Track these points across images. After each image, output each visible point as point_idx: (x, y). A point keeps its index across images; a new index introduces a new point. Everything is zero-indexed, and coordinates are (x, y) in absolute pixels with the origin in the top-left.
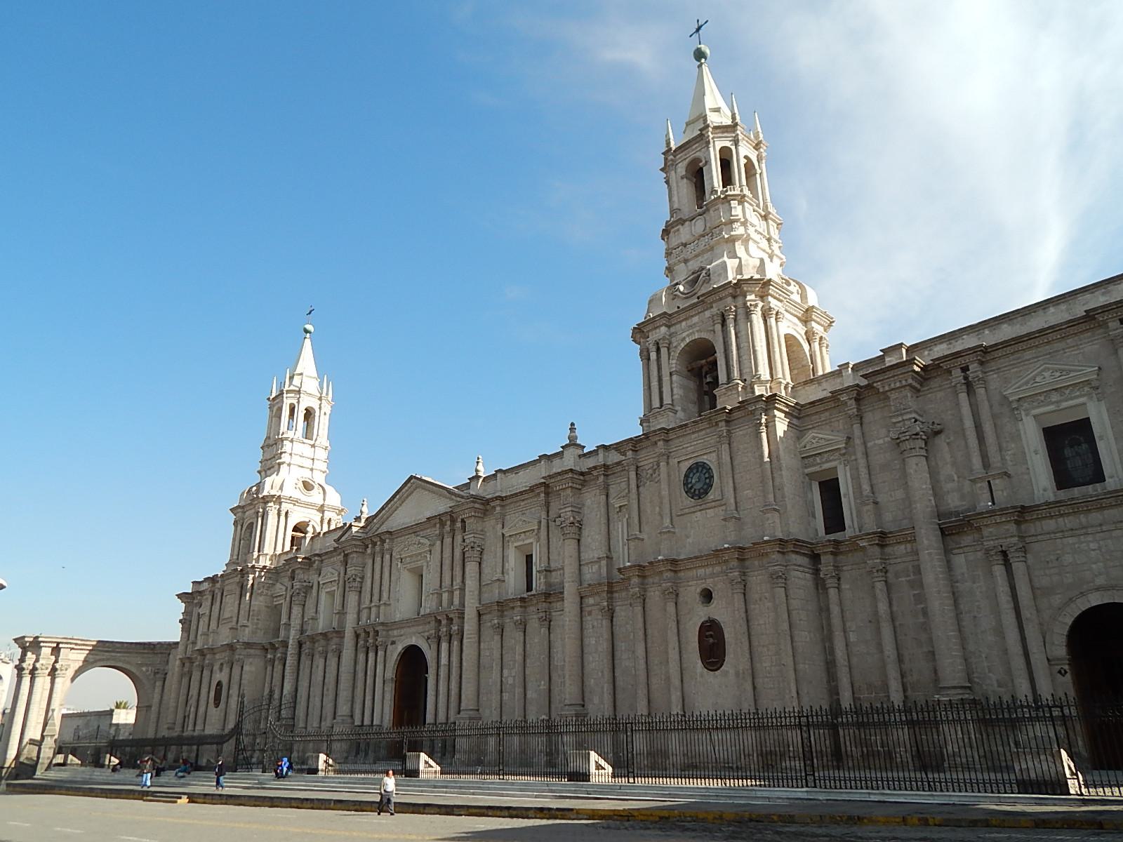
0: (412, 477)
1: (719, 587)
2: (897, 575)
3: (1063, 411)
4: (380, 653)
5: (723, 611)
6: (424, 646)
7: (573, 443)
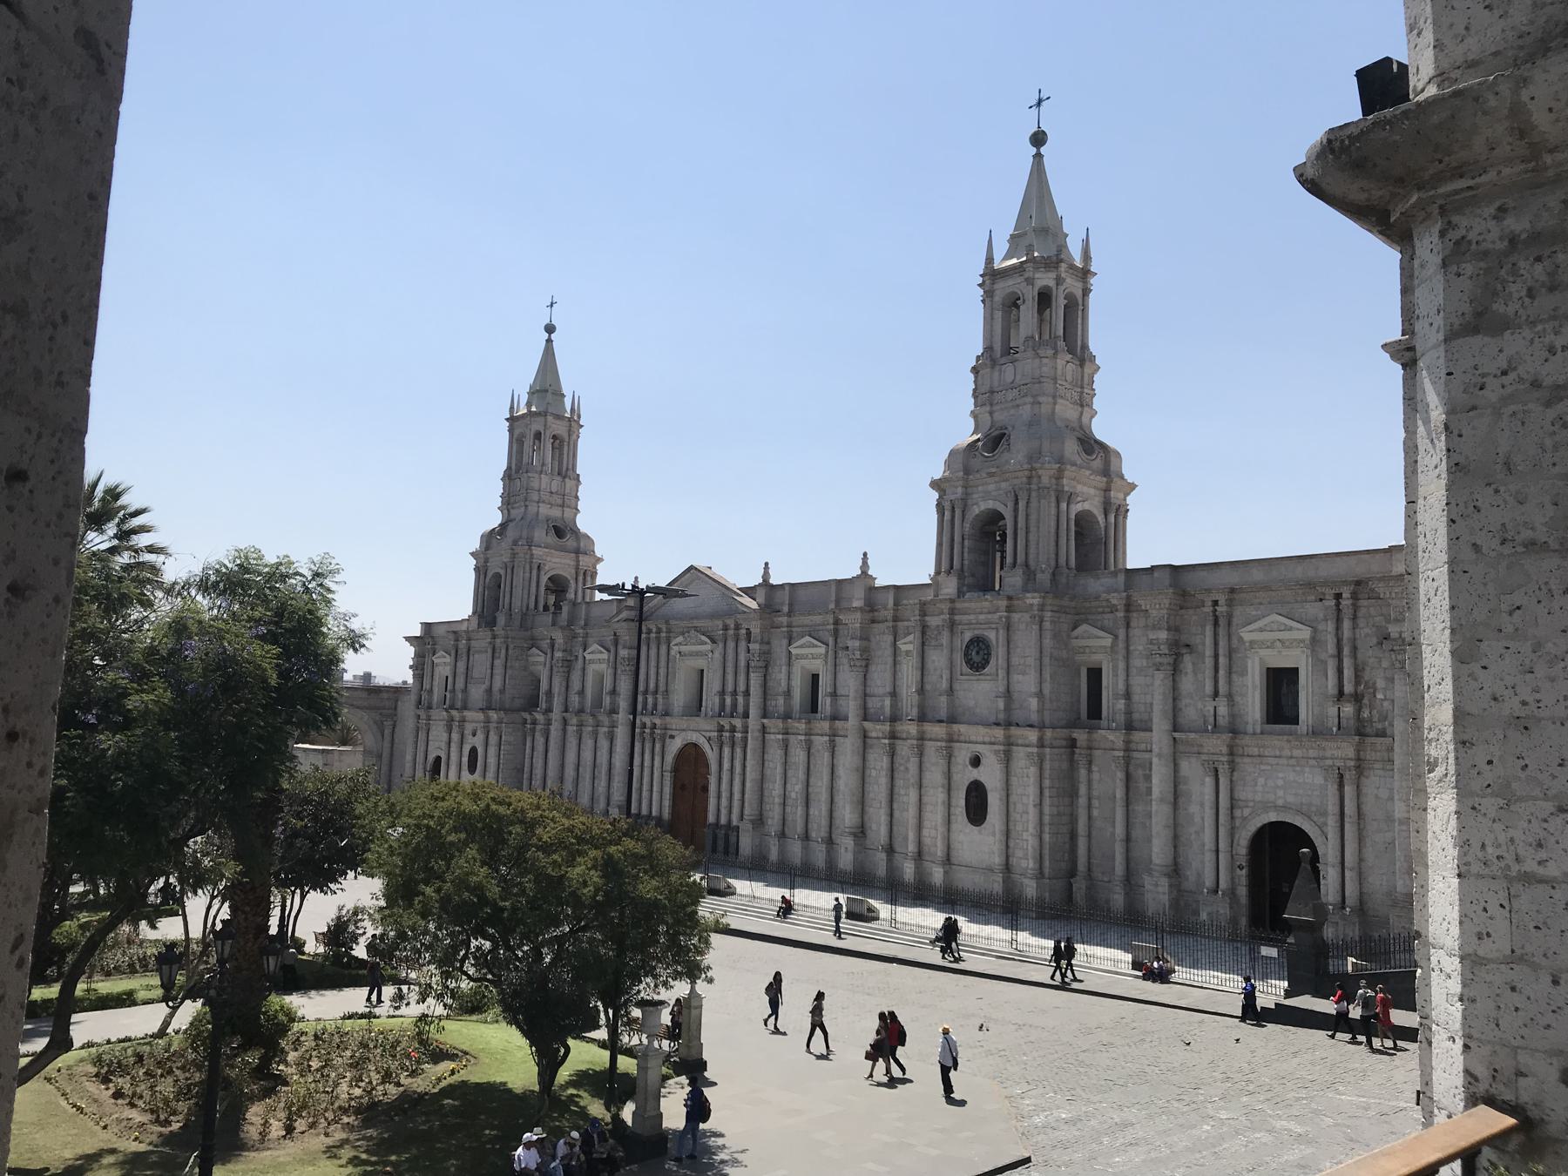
0: (692, 568)
5: (990, 775)
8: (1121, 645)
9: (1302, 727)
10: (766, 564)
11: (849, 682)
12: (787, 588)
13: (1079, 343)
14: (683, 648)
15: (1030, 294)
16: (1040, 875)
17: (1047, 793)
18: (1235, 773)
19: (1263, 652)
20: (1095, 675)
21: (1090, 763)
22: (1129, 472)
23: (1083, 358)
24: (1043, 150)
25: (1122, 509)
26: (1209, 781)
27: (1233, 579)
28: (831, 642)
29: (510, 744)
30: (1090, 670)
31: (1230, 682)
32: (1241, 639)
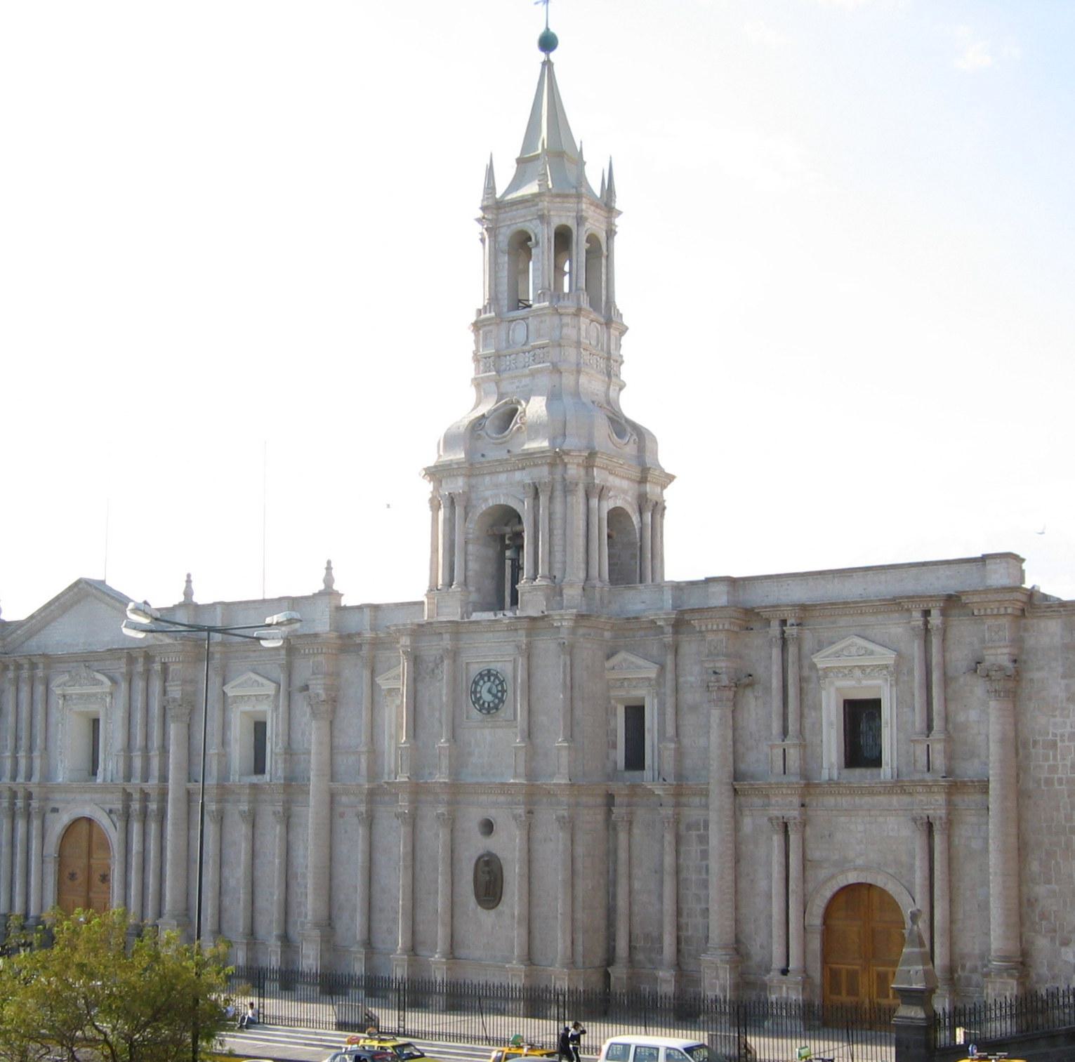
1: (500, 817)
2: (689, 828)
3: (862, 689)
4: (36, 823)
6: (104, 821)
7: (329, 592)
8: (669, 676)
9: (886, 771)
10: (189, 576)
11: (312, 735)
12: (219, 610)
13: (604, 298)
14: (69, 691)
15: (544, 236)
16: (572, 963)
18: (808, 828)
19: (841, 683)
20: (635, 715)
21: (631, 823)
22: (667, 459)
23: (610, 319)
24: (553, 56)
25: (659, 507)
26: (777, 840)
27: (799, 594)
28: (282, 678)
30: (628, 709)
31: (802, 716)
32: (813, 667)
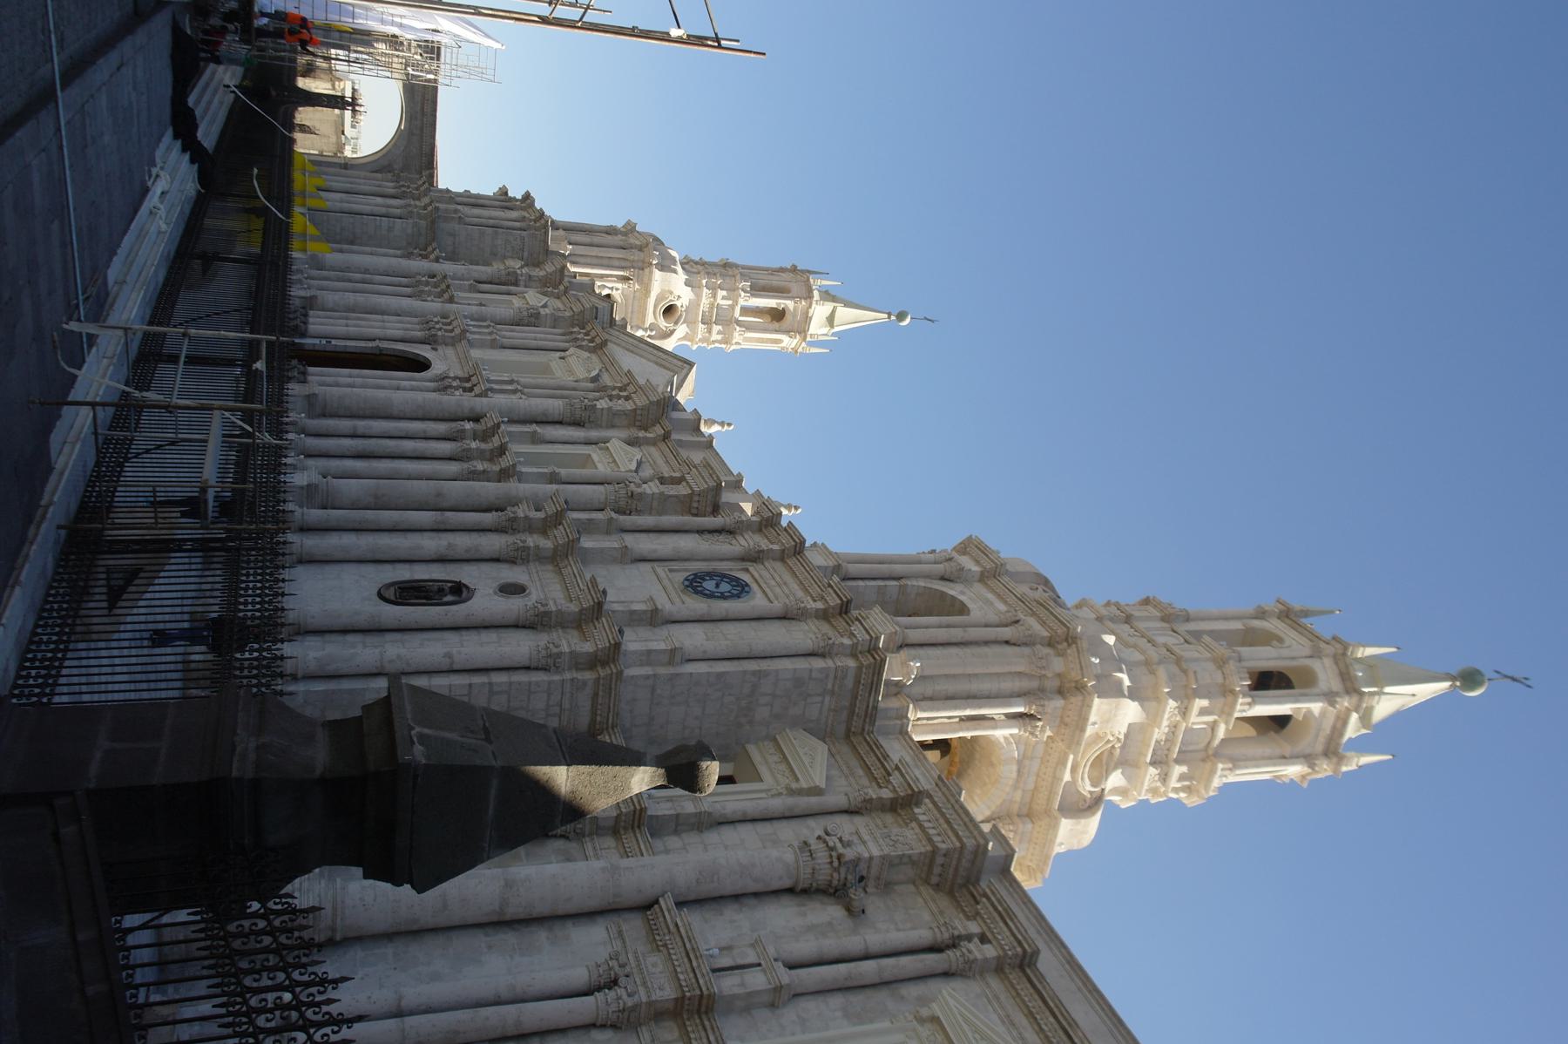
17: (477, 679)
26: (579, 975)
29: (390, 229)
